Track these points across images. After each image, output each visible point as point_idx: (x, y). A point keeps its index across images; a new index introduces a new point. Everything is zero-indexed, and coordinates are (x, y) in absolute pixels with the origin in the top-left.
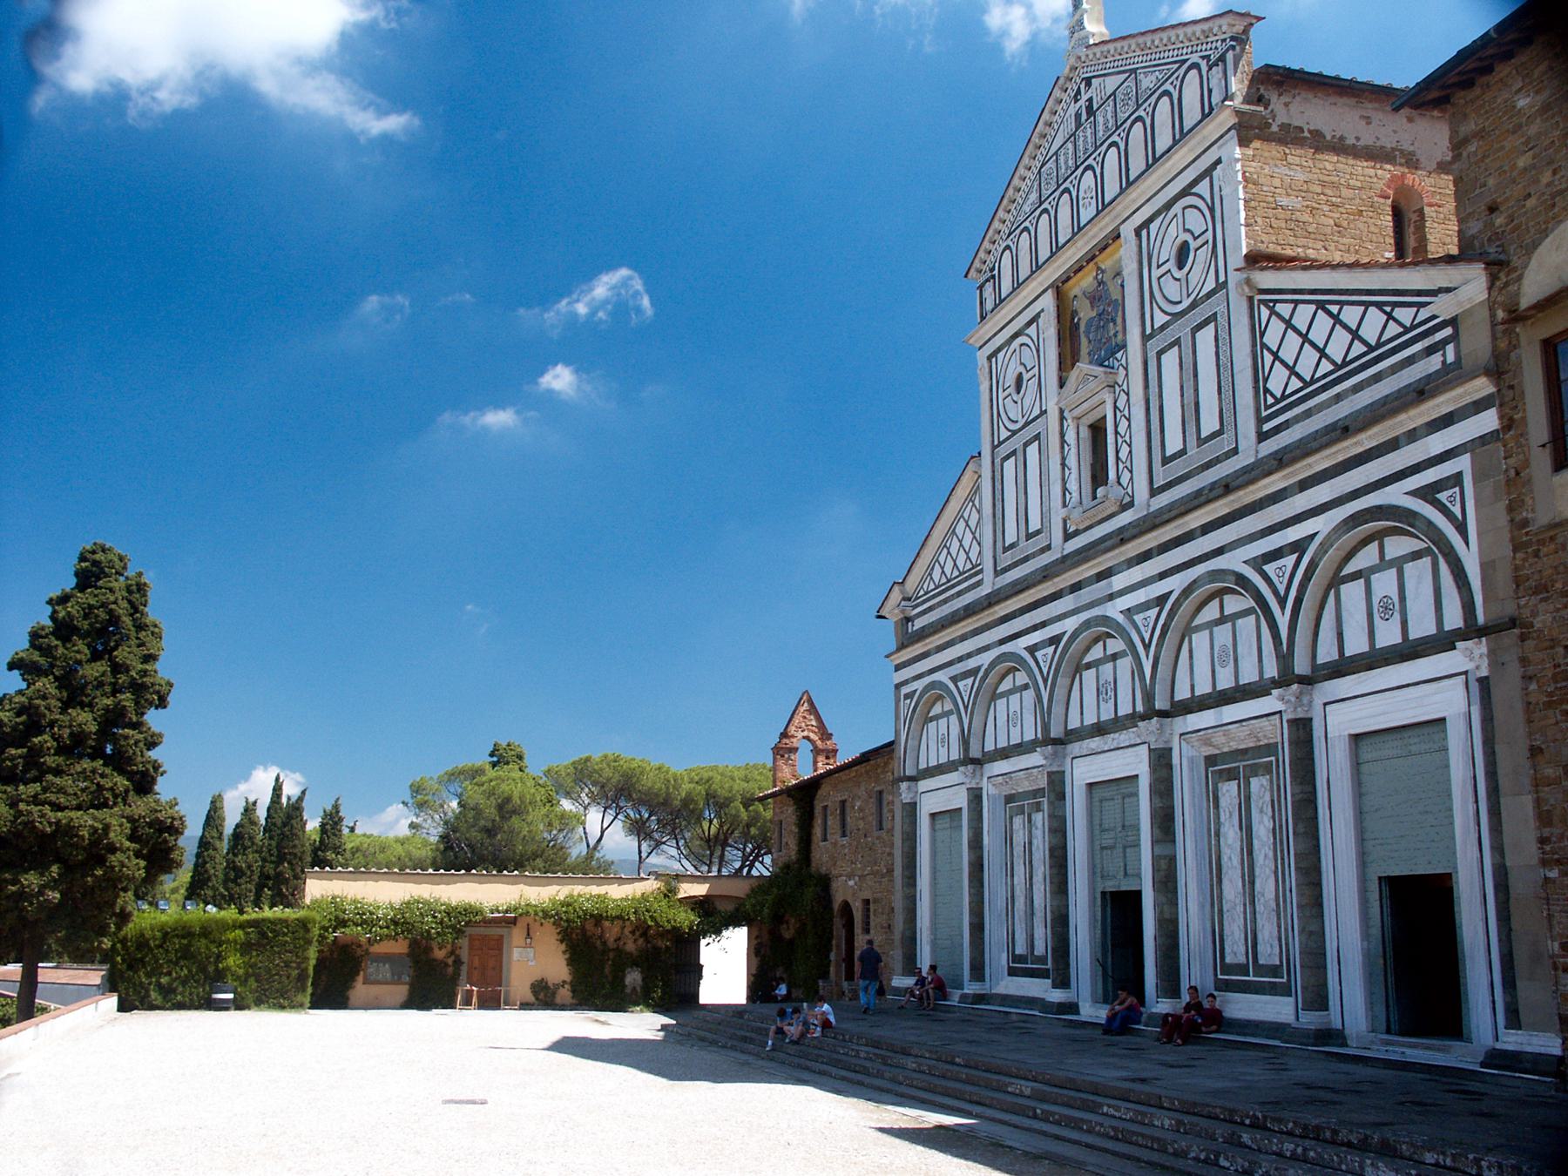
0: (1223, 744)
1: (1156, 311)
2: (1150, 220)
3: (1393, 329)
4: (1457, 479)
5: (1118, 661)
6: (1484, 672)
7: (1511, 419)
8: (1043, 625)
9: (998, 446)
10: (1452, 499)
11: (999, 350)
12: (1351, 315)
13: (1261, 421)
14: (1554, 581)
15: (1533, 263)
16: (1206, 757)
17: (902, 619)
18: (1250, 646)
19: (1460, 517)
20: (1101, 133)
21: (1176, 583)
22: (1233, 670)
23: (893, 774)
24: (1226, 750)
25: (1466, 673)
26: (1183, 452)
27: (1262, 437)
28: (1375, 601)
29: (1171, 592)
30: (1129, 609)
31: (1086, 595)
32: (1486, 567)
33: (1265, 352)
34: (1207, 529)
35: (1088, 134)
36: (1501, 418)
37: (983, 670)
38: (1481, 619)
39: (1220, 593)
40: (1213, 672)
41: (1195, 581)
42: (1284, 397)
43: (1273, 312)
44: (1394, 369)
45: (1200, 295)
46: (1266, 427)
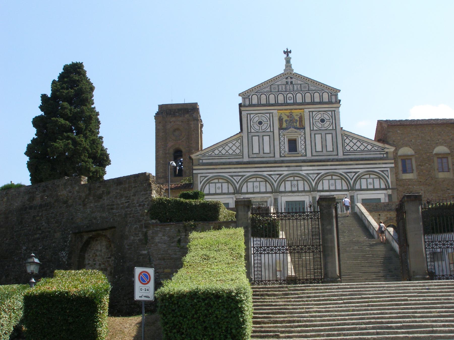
2: (314, 111)
3: (373, 149)
4: (387, 171)
5: (298, 181)
9: (249, 132)
11: (252, 114)
12: (366, 145)
13: (343, 153)
17: (198, 159)
21: (323, 172)
22: (334, 187)
26: (322, 151)
27: (344, 155)
28: (368, 182)
29: (321, 173)
30: (307, 173)
31: (292, 168)
32: (391, 182)
33: (345, 143)
34: (331, 165)
35: (291, 87)
36: (395, 165)
37: (246, 176)
38: (390, 187)
39: (332, 175)
40: (329, 187)
42: (349, 151)
43: (347, 138)
44: (373, 154)
45: (328, 129)
46: (345, 154)
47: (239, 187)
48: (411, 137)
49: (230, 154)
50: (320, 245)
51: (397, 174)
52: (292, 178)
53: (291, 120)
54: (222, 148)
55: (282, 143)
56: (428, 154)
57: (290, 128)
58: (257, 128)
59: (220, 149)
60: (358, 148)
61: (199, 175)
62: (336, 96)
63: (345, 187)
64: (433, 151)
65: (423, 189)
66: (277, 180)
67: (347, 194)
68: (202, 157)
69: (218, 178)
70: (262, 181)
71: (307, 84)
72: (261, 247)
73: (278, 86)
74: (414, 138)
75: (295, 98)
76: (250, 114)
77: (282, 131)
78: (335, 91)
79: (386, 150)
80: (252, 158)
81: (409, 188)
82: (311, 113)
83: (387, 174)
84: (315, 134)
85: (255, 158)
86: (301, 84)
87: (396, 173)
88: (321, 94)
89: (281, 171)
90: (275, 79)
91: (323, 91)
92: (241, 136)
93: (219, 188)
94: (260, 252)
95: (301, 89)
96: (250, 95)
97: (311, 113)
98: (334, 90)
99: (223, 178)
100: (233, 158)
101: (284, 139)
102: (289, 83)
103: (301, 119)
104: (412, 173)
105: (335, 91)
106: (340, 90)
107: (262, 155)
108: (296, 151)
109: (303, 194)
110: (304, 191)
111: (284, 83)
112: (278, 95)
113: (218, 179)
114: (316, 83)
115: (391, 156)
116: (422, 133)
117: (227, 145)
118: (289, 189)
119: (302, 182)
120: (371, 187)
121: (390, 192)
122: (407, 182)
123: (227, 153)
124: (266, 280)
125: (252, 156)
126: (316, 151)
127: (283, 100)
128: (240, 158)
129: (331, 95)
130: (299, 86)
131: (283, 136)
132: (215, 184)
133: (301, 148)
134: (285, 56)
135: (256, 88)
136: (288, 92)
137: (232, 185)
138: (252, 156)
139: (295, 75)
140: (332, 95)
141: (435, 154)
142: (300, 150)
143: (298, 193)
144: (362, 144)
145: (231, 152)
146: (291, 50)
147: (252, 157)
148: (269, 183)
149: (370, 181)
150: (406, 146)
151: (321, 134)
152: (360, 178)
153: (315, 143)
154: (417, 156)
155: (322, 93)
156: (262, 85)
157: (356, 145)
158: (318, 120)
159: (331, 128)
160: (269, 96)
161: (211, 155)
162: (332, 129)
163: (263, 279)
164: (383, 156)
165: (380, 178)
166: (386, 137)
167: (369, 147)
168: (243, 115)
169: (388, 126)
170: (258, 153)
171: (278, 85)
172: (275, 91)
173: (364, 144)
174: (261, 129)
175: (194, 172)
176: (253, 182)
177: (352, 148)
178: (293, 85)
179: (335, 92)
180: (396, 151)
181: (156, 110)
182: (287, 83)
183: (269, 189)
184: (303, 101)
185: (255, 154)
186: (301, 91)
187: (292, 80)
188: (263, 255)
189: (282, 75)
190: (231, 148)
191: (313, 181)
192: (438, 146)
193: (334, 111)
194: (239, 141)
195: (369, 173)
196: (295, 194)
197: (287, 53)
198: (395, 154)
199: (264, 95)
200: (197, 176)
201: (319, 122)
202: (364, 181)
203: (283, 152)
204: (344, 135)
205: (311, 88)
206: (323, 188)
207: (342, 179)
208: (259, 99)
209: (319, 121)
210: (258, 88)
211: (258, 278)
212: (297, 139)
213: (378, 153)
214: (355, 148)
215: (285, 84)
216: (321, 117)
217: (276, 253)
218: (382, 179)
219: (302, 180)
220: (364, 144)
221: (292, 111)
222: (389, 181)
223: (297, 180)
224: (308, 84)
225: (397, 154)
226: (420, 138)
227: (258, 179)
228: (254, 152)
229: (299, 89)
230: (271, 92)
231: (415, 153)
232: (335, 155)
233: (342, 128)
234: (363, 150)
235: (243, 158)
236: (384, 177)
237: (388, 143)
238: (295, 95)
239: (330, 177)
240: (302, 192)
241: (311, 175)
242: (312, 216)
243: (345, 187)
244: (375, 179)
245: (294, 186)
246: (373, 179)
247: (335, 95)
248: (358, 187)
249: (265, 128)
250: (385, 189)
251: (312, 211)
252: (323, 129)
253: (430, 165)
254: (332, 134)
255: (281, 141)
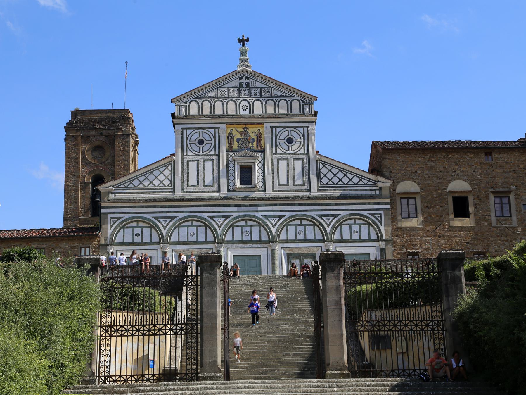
0: (296, 251)
1: (278, 149)
2: (278, 127)
3: (361, 182)
4: (380, 214)
6: (384, 247)
7: (393, 208)
8: (219, 212)
10: (379, 217)
11: (189, 128)
12: (350, 176)
13: (318, 186)
14: (401, 236)
15: (400, 184)
16: (287, 254)
18: (311, 232)
19: (380, 220)
20: (253, 94)
21: (288, 214)
23: (99, 242)
24: (296, 252)
25: (376, 247)
27: (318, 190)
30: (266, 216)
31: (243, 208)
34: (300, 205)
35: (247, 91)
38: (384, 238)
39: (301, 219)
40: (296, 235)
41: (296, 215)
42: (327, 184)
43: (324, 166)
44: (361, 190)
47: (167, 234)
48: (416, 166)
49: (155, 186)
50: (197, 324)
51: (394, 219)
52: (244, 223)
53: (246, 140)
54: (144, 177)
55: (231, 172)
56: (439, 192)
57: (244, 150)
58: (197, 149)
59: (141, 179)
60: (339, 181)
61: (109, 216)
62: (310, 105)
63: (319, 237)
64: (447, 187)
65: (430, 241)
66: (221, 224)
67: (321, 247)
68: (115, 190)
69: (137, 220)
70: (200, 226)
71: (269, 87)
72: (111, 327)
73: (228, 89)
74: (420, 168)
75: (251, 108)
76: (186, 129)
77: (231, 154)
78: (310, 98)
79: (380, 185)
80: (187, 192)
81: (411, 239)
82: (274, 129)
83: (380, 219)
84: (278, 160)
85: (192, 192)
86: (261, 88)
87: (392, 218)
88: (289, 103)
89: (229, 212)
90: (224, 79)
91: (293, 98)
92: (172, 161)
93: (137, 235)
94: (110, 333)
95: (261, 95)
96: (188, 101)
97: (274, 129)
98: (308, 97)
99: (145, 220)
100: (160, 192)
101: (234, 166)
102: (244, 86)
103: (259, 136)
104: (416, 217)
105: (310, 98)
106: (317, 98)
107: (201, 189)
108: (252, 184)
109: (259, 245)
110: (260, 241)
111: (236, 85)
112: (228, 102)
113: (137, 222)
114: (283, 87)
115: (386, 192)
116: (432, 161)
117: (151, 173)
118: (238, 237)
119: (258, 227)
120: (356, 237)
121: (382, 244)
122: (408, 230)
123: (151, 185)
124: (116, 374)
125: (186, 189)
126: (279, 185)
127: (234, 109)
128: (169, 192)
129: (303, 105)
130: (258, 91)
131: (233, 162)
132: (131, 229)
133: (258, 178)
134: (240, 45)
135: (196, 91)
136: (243, 99)
137: (157, 231)
138: (186, 189)
139: (253, 74)
140: (306, 104)
141: (449, 191)
142: (256, 182)
143: (251, 245)
144: (345, 175)
145: (156, 183)
146: (248, 38)
147: (187, 190)
148: (155, 229)
149: (355, 228)
150: (409, 179)
151: (287, 160)
152: (341, 224)
153: (278, 173)
154: (423, 193)
155: (290, 101)
156: (206, 88)
157: (337, 177)
158: (284, 139)
159: (302, 151)
160: (214, 104)
161: (127, 187)
162: (303, 152)
163: (112, 374)
164: (375, 192)
165: (369, 224)
166: (381, 166)
167: (356, 180)
168: (177, 130)
169: (384, 149)
170: (196, 184)
171: (228, 88)
172: (223, 97)
173: (348, 175)
174: (201, 152)
175: (103, 211)
176: (188, 227)
177: (330, 180)
178: (250, 88)
179: (309, 100)
180: (393, 187)
181: (68, 118)
182: (241, 85)
183: (210, 238)
184: (263, 112)
185: (192, 186)
186: (261, 97)
187: (248, 81)
188: (113, 339)
189: (234, 74)
190: (156, 177)
191: (274, 226)
192: (454, 180)
193: (308, 127)
194: (169, 167)
195: (354, 217)
196: (247, 245)
197: (243, 41)
198: (392, 190)
199: (207, 102)
200: (107, 218)
201: (284, 142)
202: (346, 229)
203: (231, 184)
204: (320, 162)
205: (275, 93)
206: (287, 238)
207: (315, 225)
208: (200, 108)
209: (285, 141)
210: (198, 91)
211: (104, 372)
212: (253, 166)
213: (368, 188)
214: (335, 180)
215: (239, 86)
216: (288, 135)
217: (154, 335)
218: (372, 226)
219: (258, 226)
220: (348, 175)
221: (247, 126)
222: (383, 229)
223: (251, 226)
224: (271, 88)
225: (395, 190)
226: (429, 168)
227: (195, 223)
228: (190, 185)
229: (258, 94)
230: (217, 98)
231: (421, 189)
232: (305, 191)
233: (317, 152)
234: (347, 184)
235: (174, 192)
236: (375, 224)
237: (382, 175)
238: (251, 104)
239: (298, 222)
240: (257, 242)
241: (270, 219)
242: (188, 282)
243: (319, 237)
244: (362, 226)
245: (246, 234)
246: (360, 225)
247: (309, 104)
248: (337, 236)
249: (207, 149)
250: (377, 240)
251: (194, 274)
252: (291, 152)
253: (441, 206)
254: (303, 160)
255: (229, 169)
